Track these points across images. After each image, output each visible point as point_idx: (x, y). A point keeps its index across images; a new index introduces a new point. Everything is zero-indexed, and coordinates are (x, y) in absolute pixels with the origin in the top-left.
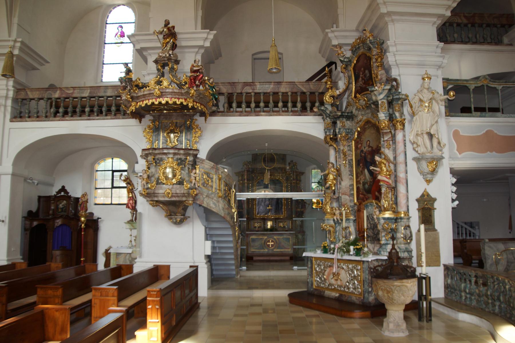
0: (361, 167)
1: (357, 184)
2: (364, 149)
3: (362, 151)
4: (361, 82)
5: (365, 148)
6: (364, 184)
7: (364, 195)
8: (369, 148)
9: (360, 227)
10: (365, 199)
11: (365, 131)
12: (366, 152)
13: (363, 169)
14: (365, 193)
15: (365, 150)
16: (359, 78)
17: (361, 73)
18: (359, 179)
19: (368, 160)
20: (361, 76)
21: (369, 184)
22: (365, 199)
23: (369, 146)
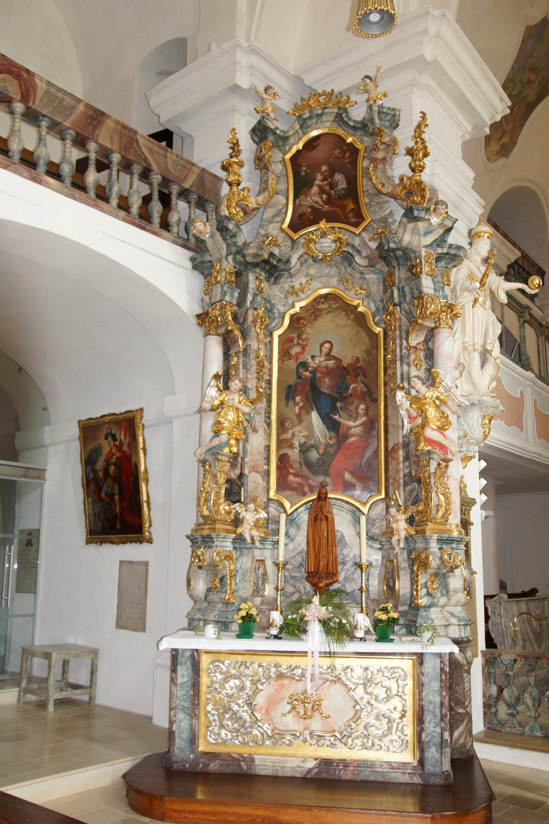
0: (296, 404)
1: (278, 448)
2: (310, 360)
3: (304, 365)
5: (313, 357)
6: (305, 449)
8: (326, 360)
10: (306, 489)
11: (316, 317)
12: (314, 372)
13: (306, 409)
15: (313, 364)
17: (319, 177)
18: (289, 435)
19: (325, 389)
20: (317, 182)
22: (306, 489)
23: (329, 356)
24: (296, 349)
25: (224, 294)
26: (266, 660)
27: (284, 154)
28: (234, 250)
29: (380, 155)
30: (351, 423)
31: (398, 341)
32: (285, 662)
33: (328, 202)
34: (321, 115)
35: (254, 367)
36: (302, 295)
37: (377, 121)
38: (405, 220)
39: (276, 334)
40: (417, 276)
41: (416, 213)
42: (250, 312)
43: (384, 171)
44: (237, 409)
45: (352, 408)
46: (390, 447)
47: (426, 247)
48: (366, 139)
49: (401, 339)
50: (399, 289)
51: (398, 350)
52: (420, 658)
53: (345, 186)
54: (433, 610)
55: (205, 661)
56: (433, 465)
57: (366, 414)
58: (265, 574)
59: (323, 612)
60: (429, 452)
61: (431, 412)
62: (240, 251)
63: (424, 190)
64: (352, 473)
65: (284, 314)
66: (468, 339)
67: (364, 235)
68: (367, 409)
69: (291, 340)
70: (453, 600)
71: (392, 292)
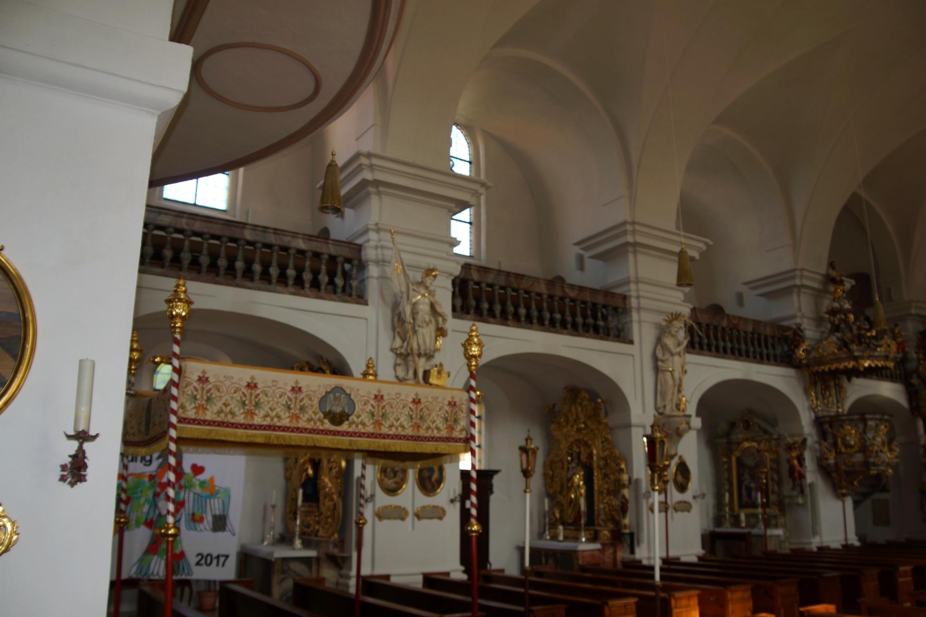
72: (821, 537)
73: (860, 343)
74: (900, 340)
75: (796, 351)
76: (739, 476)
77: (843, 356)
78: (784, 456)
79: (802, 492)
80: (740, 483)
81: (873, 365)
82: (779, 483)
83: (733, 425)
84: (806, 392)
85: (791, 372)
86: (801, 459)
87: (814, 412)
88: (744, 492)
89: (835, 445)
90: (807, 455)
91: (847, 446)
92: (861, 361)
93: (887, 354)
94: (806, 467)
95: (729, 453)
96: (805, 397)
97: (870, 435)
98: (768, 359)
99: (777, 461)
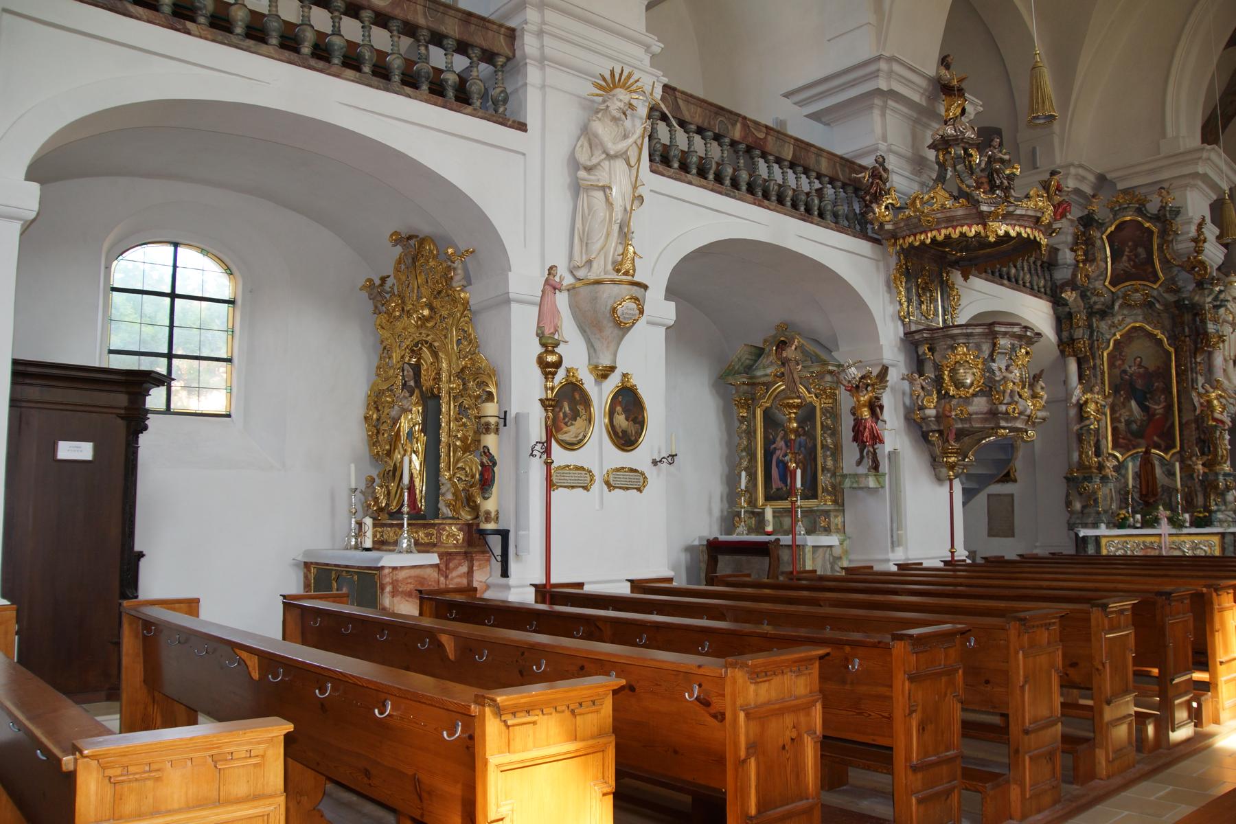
0: (1121, 396)
2: (1128, 369)
3: (1125, 372)
4: (1124, 263)
5: (1130, 367)
6: (1128, 423)
7: (1129, 440)
9: (1150, 489)
12: (1131, 375)
13: (1128, 399)
14: (1131, 438)
15: (1130, 371)
16: (1123, 256)
17: (1127, 250)
18: (1118, 415)
19: (1138, 386)
20: (1126, 253)
21: (1139, 424)
22: (1131, 447)
23: (1140, 366)
24: (1119, 362)
25: (1084, 334)
26: (1137, 540)
27: (1103, 234)
28: (1087, 306)
29: (1170, 238)
30: (1156, 407)
31: (1189, 359)
32: (1148, 540)
33: (1133, 267)
34: (1126, 208)
35: (1099, 377)
36: (1120, 328)
37: (1168, 216)
38: (1197, 289)
39: (1105, 354)
40: (1203, 322)
41: (1205, 286)
42: (1096, 343)
43: (1173, 249)
44: (1097, 403)
45: (1156, 398)
46: (1184, 421)
47: (1208, 303)
48: (1158, 224)
49: (1191, 358)
50: (1189, 327)
51: (1189, 365)
52: (1223, 535)
53: (1145, 256)
54: (1218, 513)
55: (1103, 541)
56: (1218, 433)
57: (1165, 401)
58: (1112, 497)
59: (1168, 513)
60: (1216, 426)
61: (1215, 402)
62: (1091, 307)
63: (1206, 268)
64: (1158, 437)
65: (1110, 340)
66: (1227, 353)
67: (1160, 289)
68: (1166, 398)
69: (1115, 357)
70: (1229, 507)
71: (1184, 329)
72: (906, 549)
73: (993, 188)
74: (1057, 199)
75: (874, 206)
76: (768, 442)
77: (960, 212)
78: (846, 401)
79: (876, 467)
80: (768, 455)
81: (1013, 234)
82: (836, 452)
83: (759, 352)
84: (890, 285)
85: (864, 246)
86: (875, 407)
87: (904, 325)
88: (775, 472)
89: (939, 381)
90: (887, 399)
91: (959, 384)
92: (993, 225)
93: (1039, 215)
94: (885, 422)
95: (749, 402)
96: (887, 296)
97: (1000, 363)
98: (821, 215)
99: (833, 413)
